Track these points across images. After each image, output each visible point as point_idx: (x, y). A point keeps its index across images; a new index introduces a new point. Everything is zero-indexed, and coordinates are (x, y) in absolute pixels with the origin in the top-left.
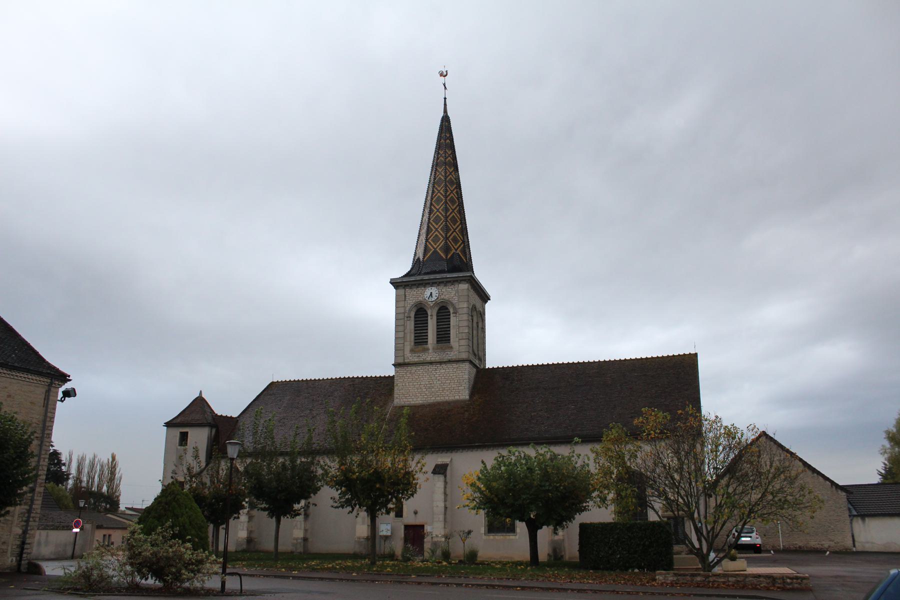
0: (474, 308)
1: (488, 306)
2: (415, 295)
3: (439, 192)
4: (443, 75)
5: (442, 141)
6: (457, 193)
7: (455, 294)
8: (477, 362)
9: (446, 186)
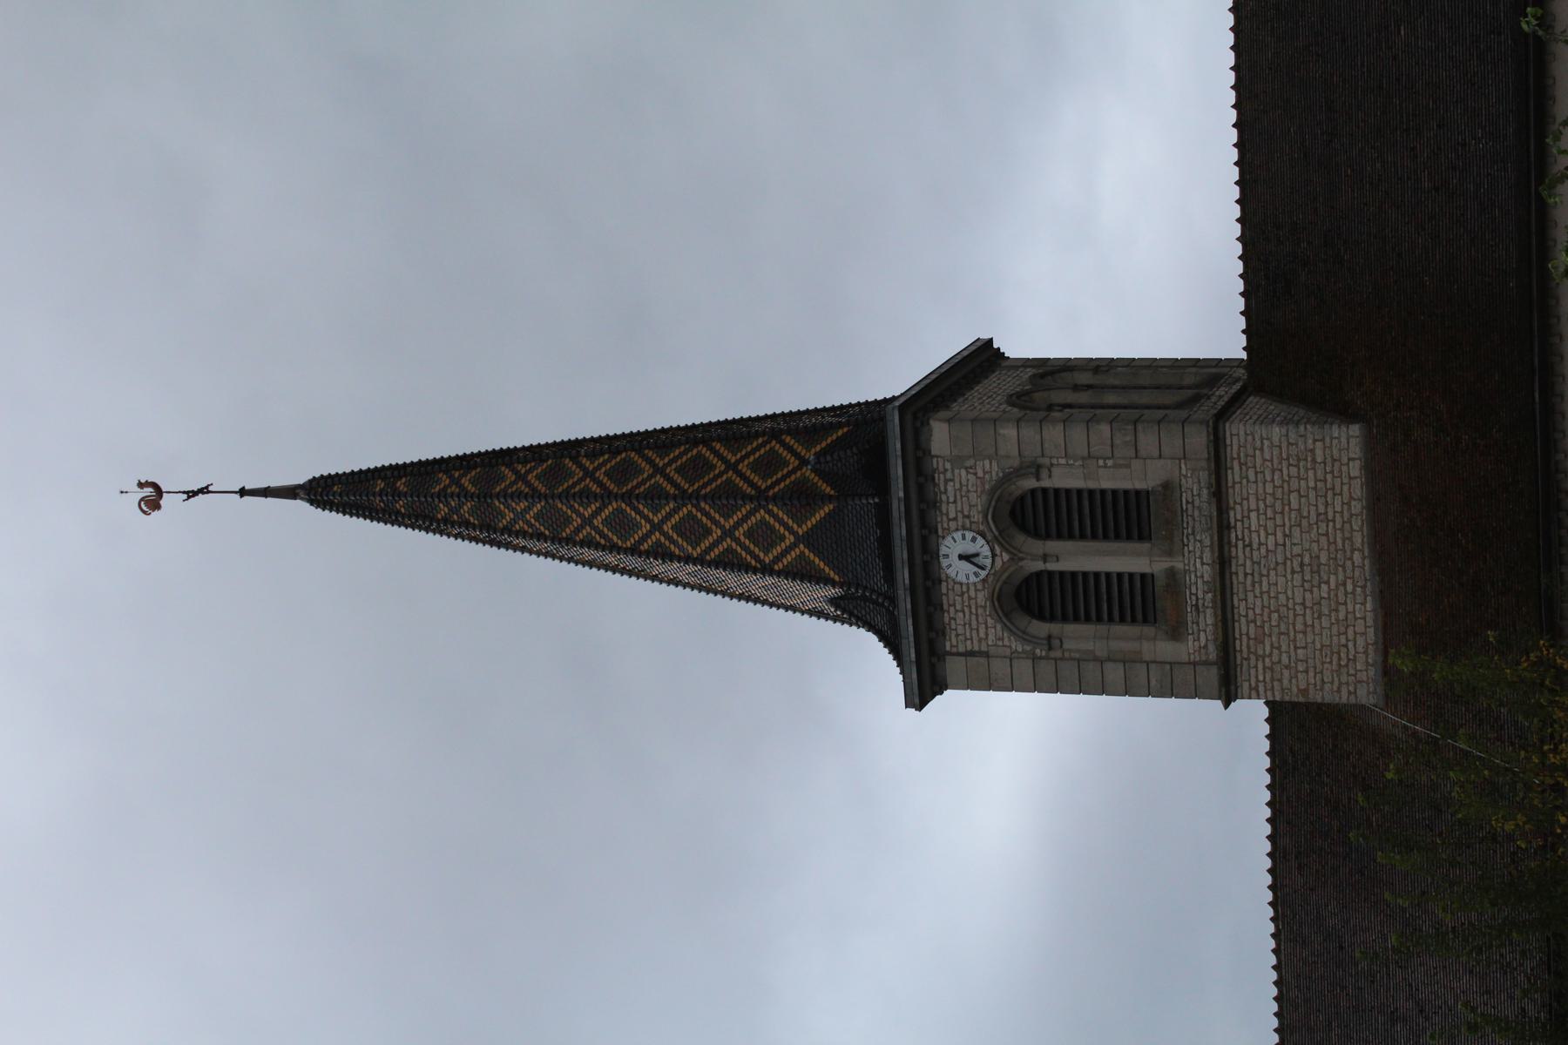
0: (1022, 401)
1: (1013, 348)
2: (970, 623)
3: (587, 521)
4: (153, 499)
5: (400, 505)
6: (592, 456)
7: (965, 466)
8: (1223, 393)
9: (567, 496)
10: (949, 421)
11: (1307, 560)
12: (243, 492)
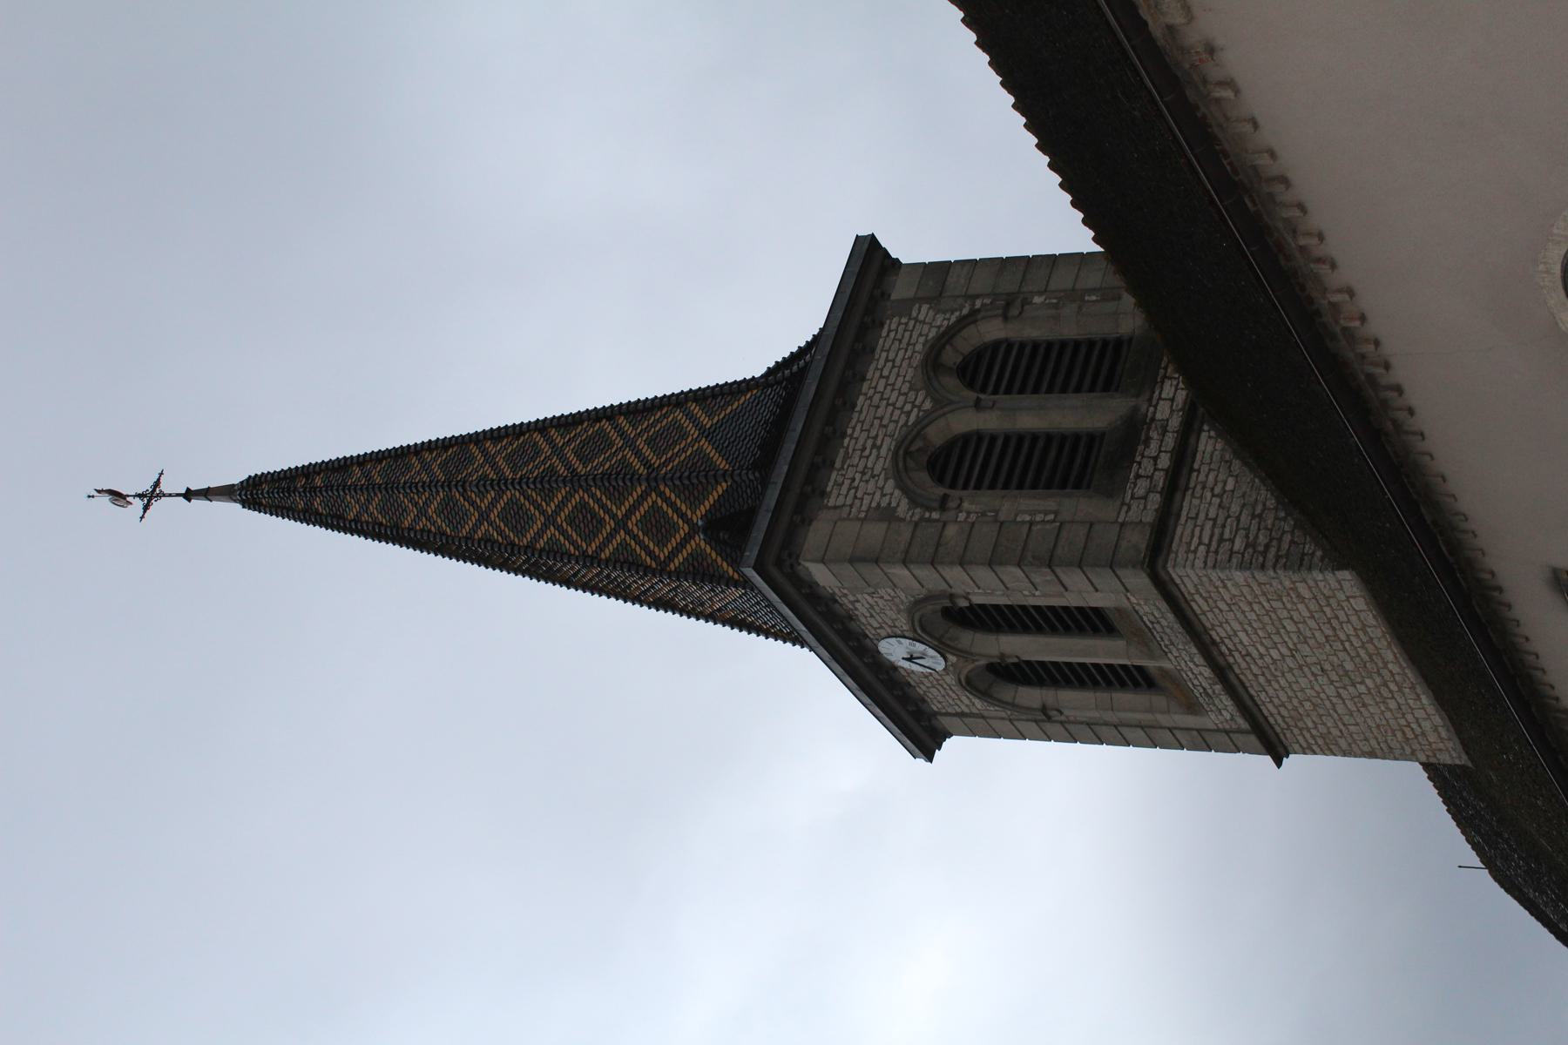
2: (944, 697)
10: (823, 561)
11: (1327, 667)
12: (189, 495)
